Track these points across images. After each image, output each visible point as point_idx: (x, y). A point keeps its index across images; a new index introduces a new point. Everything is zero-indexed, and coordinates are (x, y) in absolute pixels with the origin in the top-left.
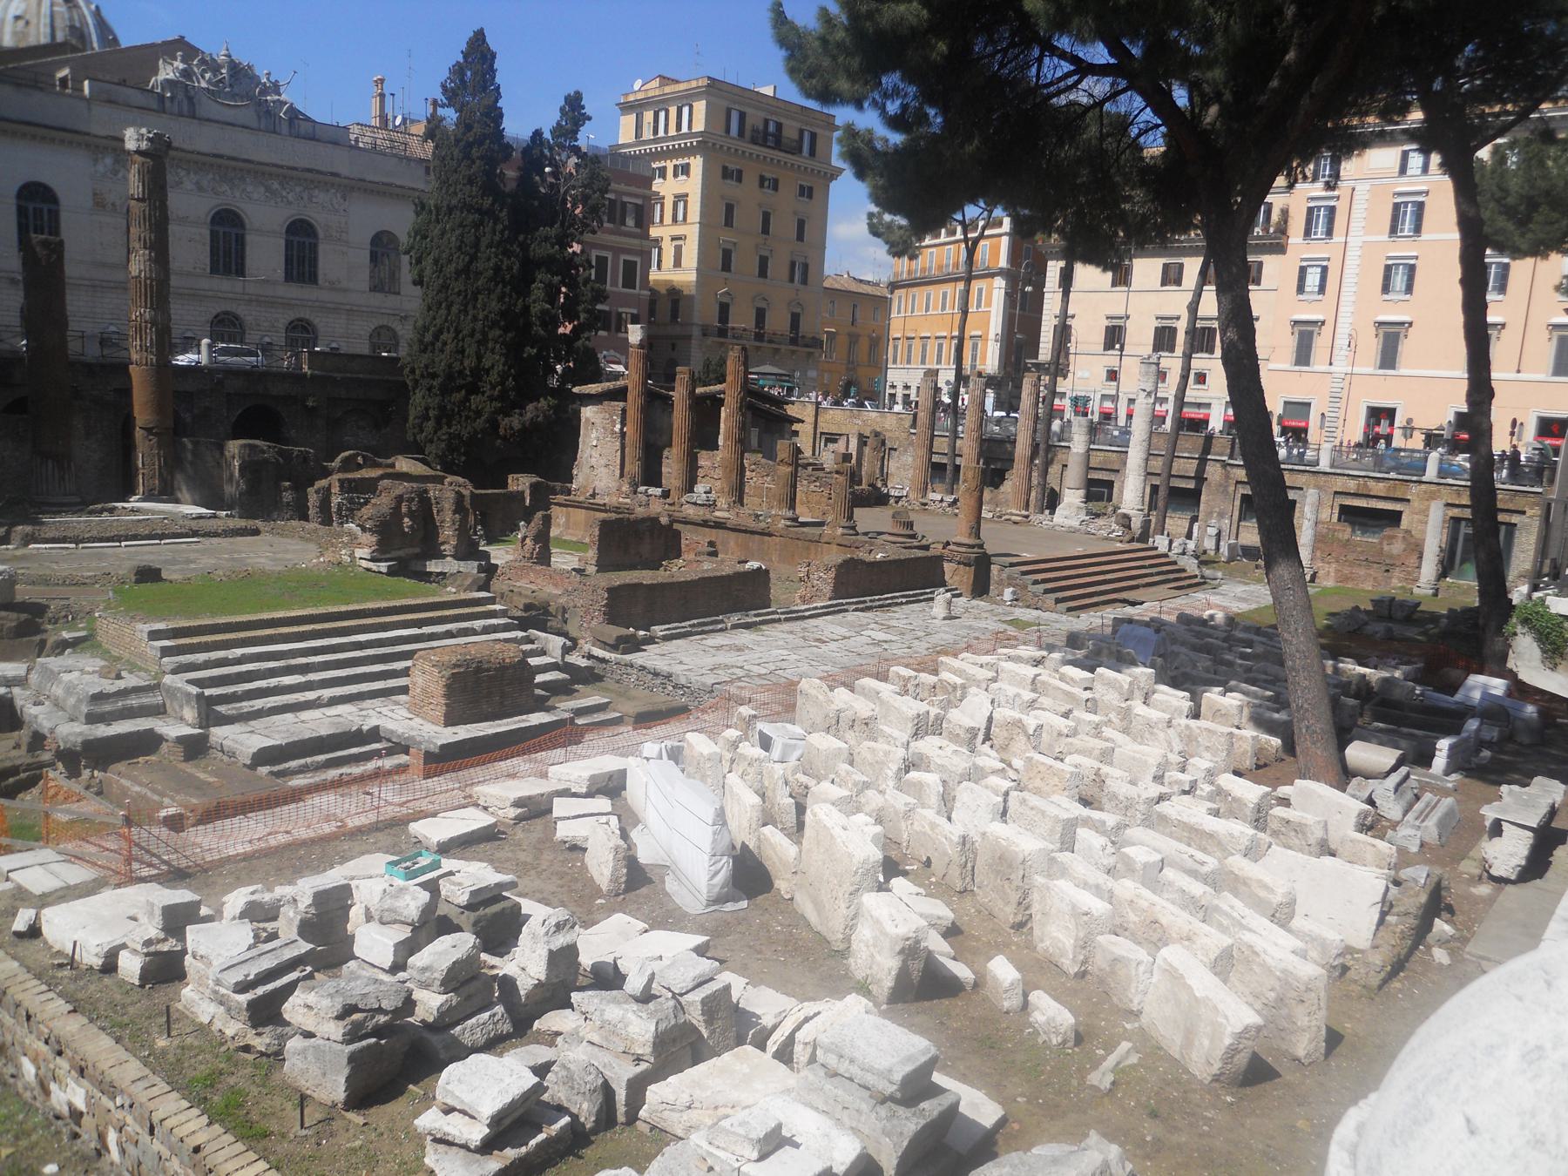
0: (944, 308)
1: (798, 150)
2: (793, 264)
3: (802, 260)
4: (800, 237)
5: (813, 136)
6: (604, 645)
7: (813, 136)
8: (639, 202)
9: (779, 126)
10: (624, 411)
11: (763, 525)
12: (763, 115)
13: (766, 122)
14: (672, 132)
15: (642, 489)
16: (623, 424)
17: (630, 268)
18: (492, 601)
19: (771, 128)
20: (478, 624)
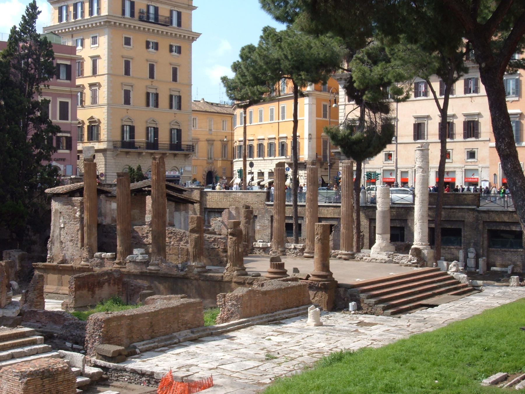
0: (272, 119)
1: (168, 23)
2: (171, 97)
4: (175, 79)
5: (179, 14)
6: (105, 358)
7: (179, 14)
8: (68, 63)
9: (156, 9)
10: (82, 203)
11: (182, 273)
14: (87, 16)
15: (98, 254)
16: (82, 212)
17: (64, 107)
19: (152, 10)
20: (26, 349)
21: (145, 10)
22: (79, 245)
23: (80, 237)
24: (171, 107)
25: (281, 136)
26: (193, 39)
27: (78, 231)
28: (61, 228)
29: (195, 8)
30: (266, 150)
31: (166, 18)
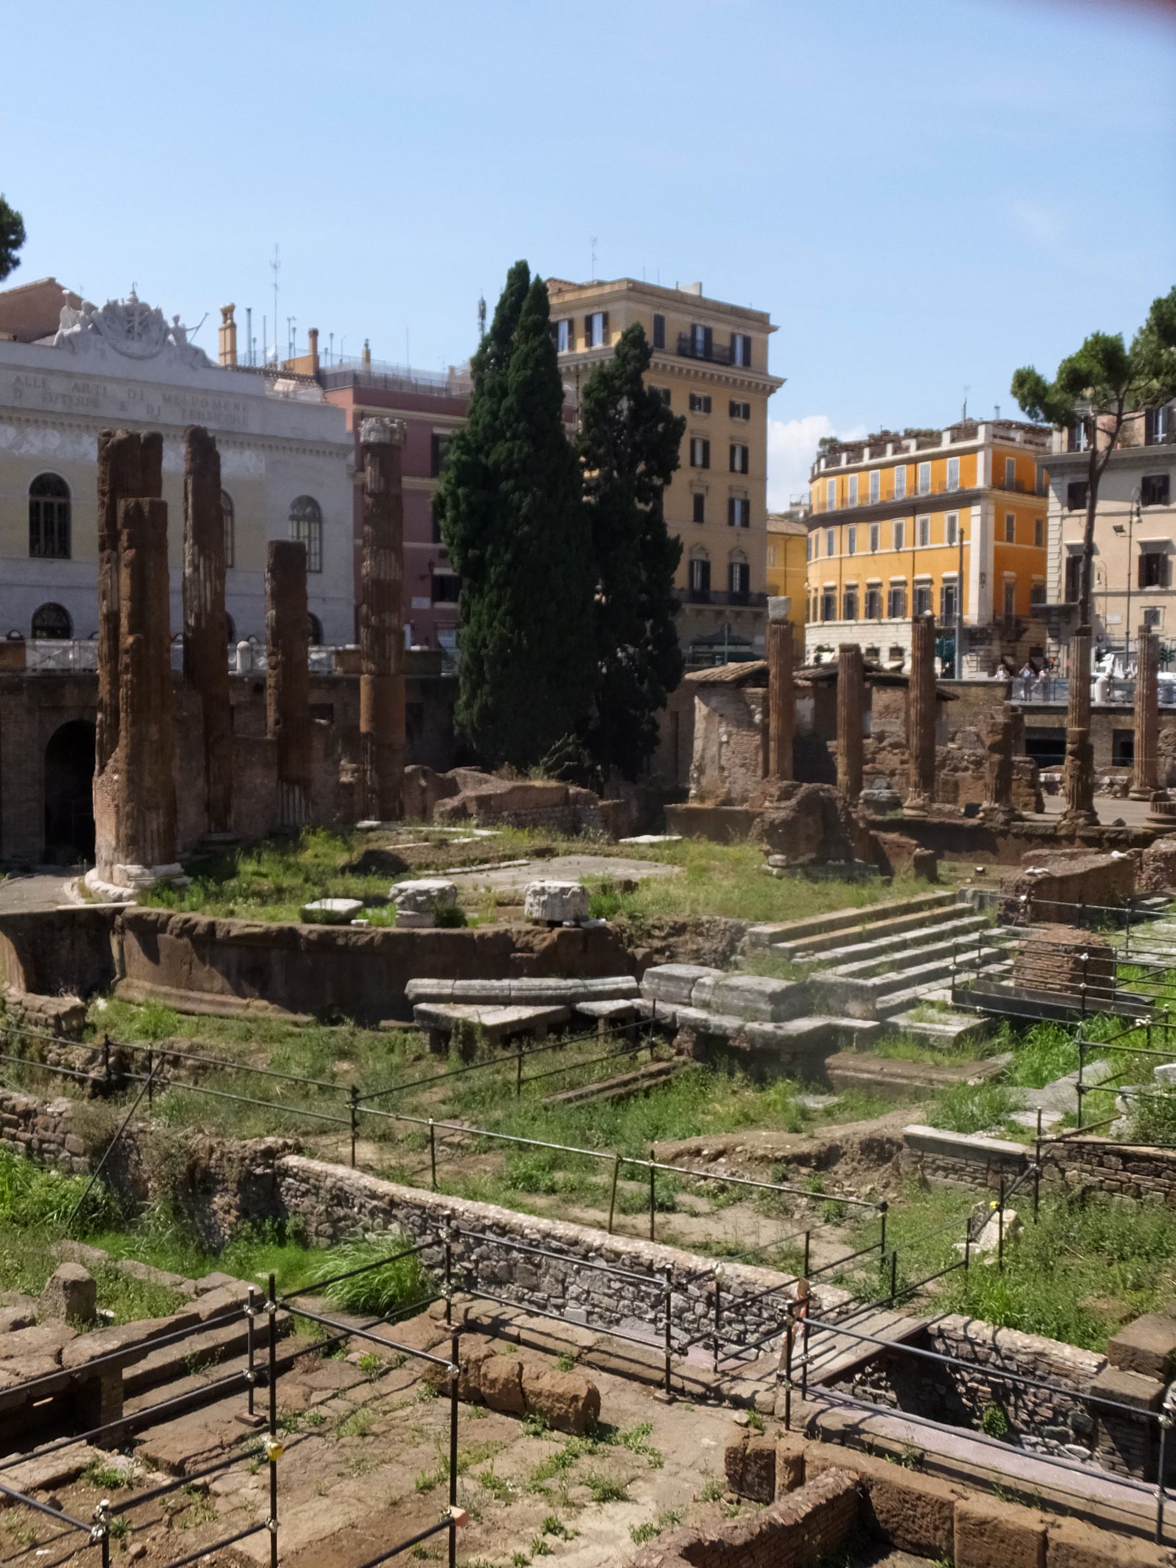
0: (899, 544)
1: (728, 361)
3: (741, 496)
7: (747, 342)
9: (708, 333)
10: (765, 698)
12: (689, 319)
13: (694, 328)
16: (766, 714)
18: (953, 899)
19: (700, 336)
21: (689, 334)
22: (760, 772)
23: (760, 759)
24: (731, 522)
25: (918, 577)
26: (772, 390)
27: (757, 748)
28: (721, 744)
29: (774, 329)
30: (862, 605)
31: (724, 349)
